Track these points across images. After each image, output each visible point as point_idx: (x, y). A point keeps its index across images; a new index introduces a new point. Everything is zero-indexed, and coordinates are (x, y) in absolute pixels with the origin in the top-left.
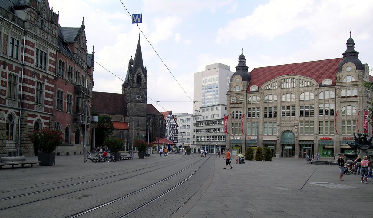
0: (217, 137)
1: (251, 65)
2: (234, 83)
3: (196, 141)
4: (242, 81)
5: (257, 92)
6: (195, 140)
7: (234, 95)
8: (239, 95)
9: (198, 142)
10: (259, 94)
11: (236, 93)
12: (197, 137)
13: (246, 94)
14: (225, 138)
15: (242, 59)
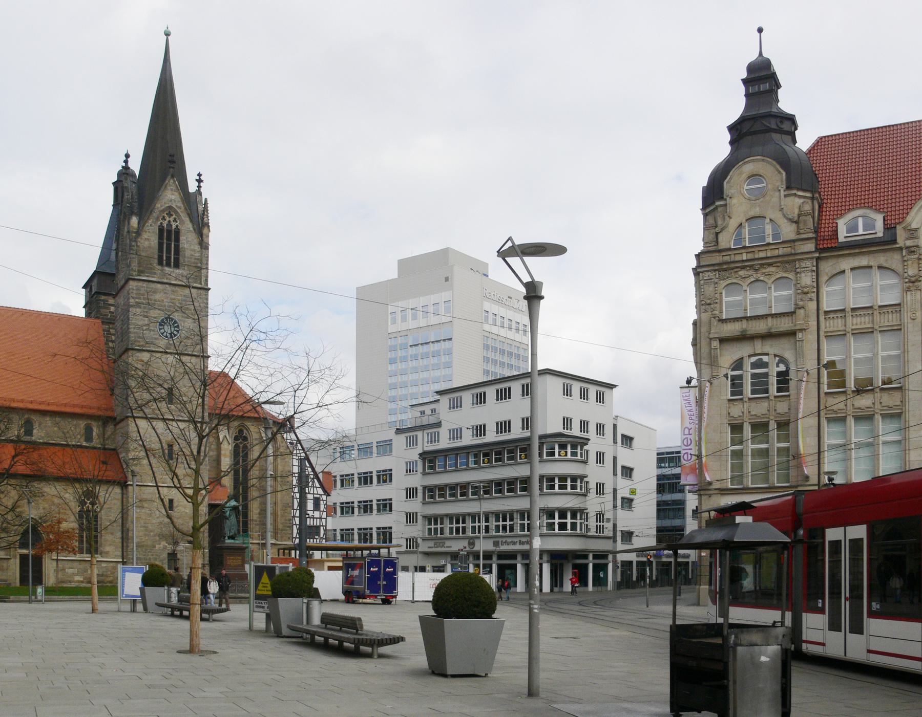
0: (458, 522)
1: (817, 114)
2: (734, 201)
3: (424, 539)
4: (788, 188)
5: (887, 242)
6: (417, 530)
7: (743, 268)
8: (772, 269)
9: (431, 544)
10: (897, 256)
11: (750, 256)
12: (429, 519)
13: (818, 259)
14: (569, 521)
15: (761, 79)
